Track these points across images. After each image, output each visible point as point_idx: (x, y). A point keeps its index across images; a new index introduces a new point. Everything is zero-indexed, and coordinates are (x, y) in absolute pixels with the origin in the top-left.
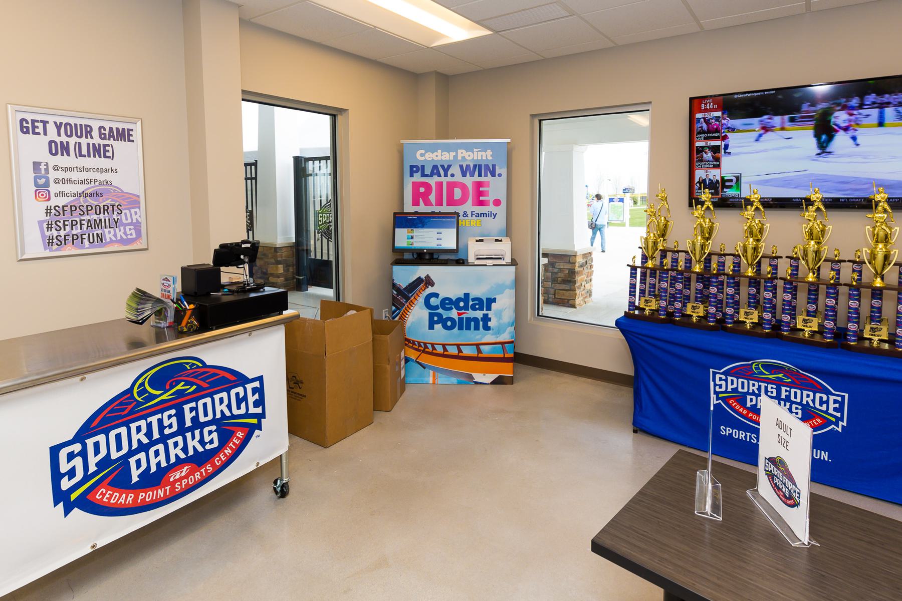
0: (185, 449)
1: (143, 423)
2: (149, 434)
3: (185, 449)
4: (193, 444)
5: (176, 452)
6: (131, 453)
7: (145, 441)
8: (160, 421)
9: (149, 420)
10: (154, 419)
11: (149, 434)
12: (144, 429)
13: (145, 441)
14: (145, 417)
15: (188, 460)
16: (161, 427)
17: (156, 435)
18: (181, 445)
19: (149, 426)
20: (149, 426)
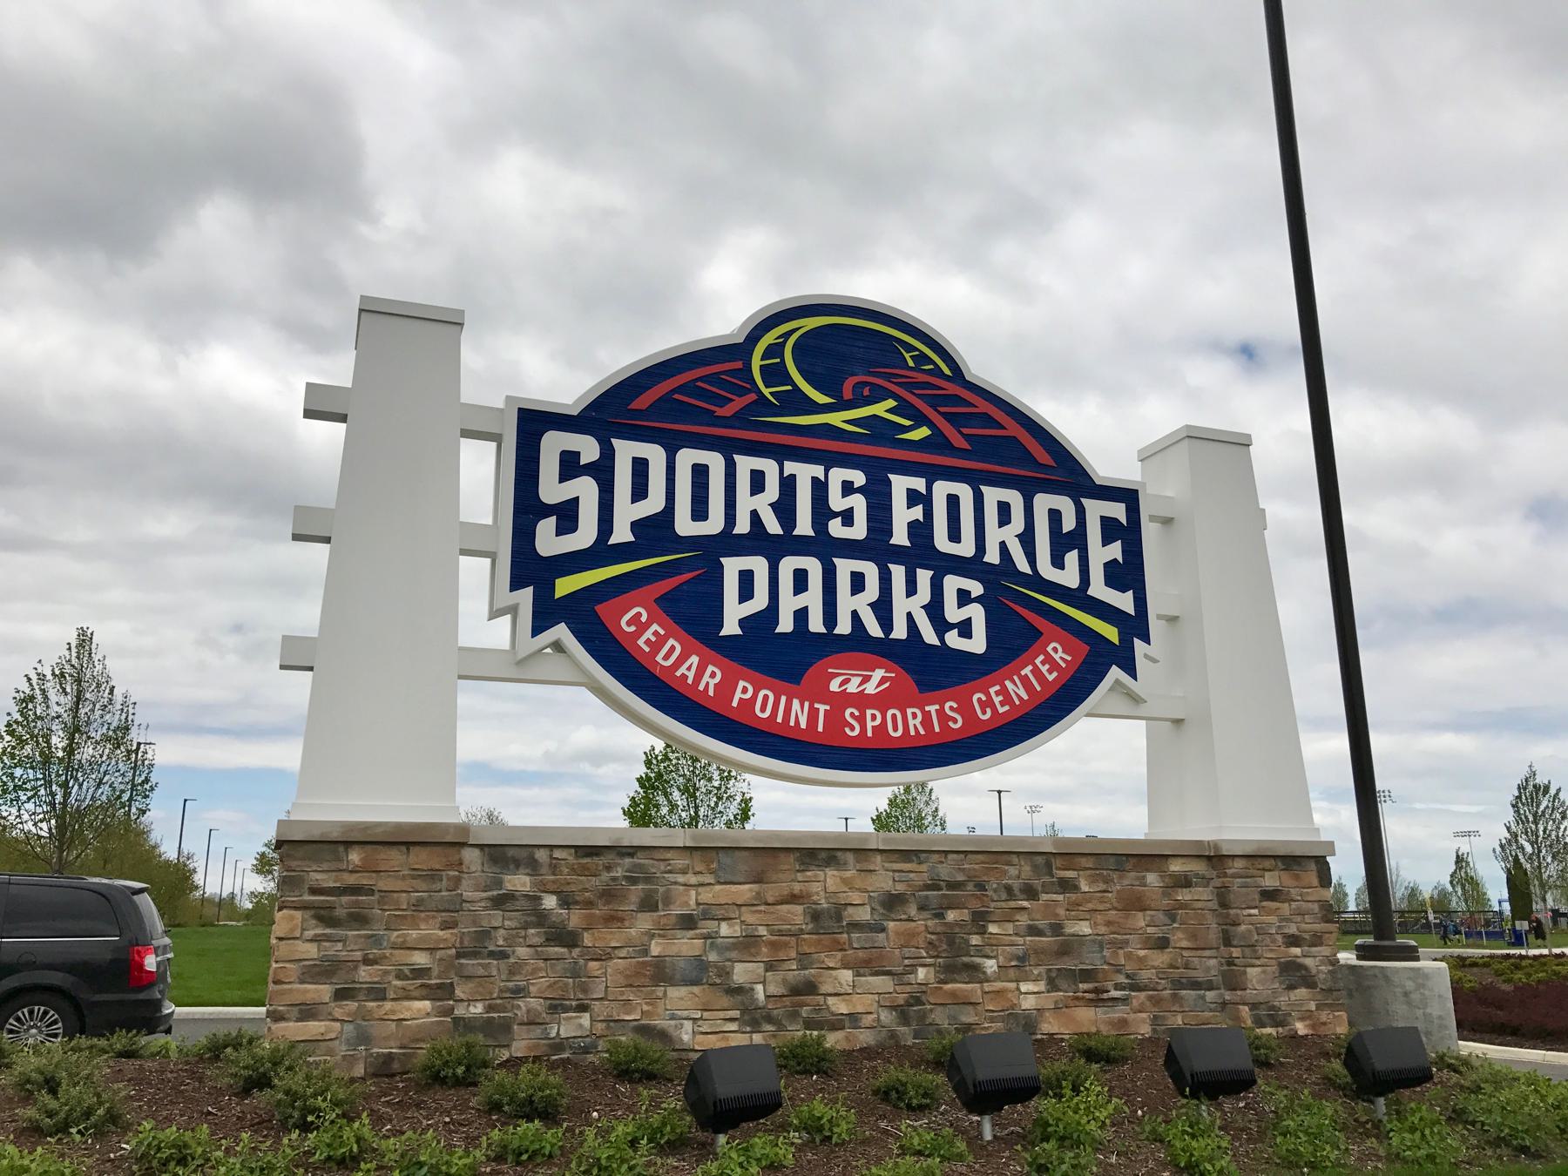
0: (883, 608)
1: (769, 466)
2: (785, 508)
4: (908, 607)
6: (728, 543)
7: (773, 526)
8: (820, 488)
9: (790, 467)
10: (805, 473)
11: (785, 508)
12: (772, 491)
13: (773, 526)
14: (781, 454)
15: (886, 650)
16: (822, 512)
17: (804, 527)
18: (872, 591)
19: (788, 484)
20: (788, 484)
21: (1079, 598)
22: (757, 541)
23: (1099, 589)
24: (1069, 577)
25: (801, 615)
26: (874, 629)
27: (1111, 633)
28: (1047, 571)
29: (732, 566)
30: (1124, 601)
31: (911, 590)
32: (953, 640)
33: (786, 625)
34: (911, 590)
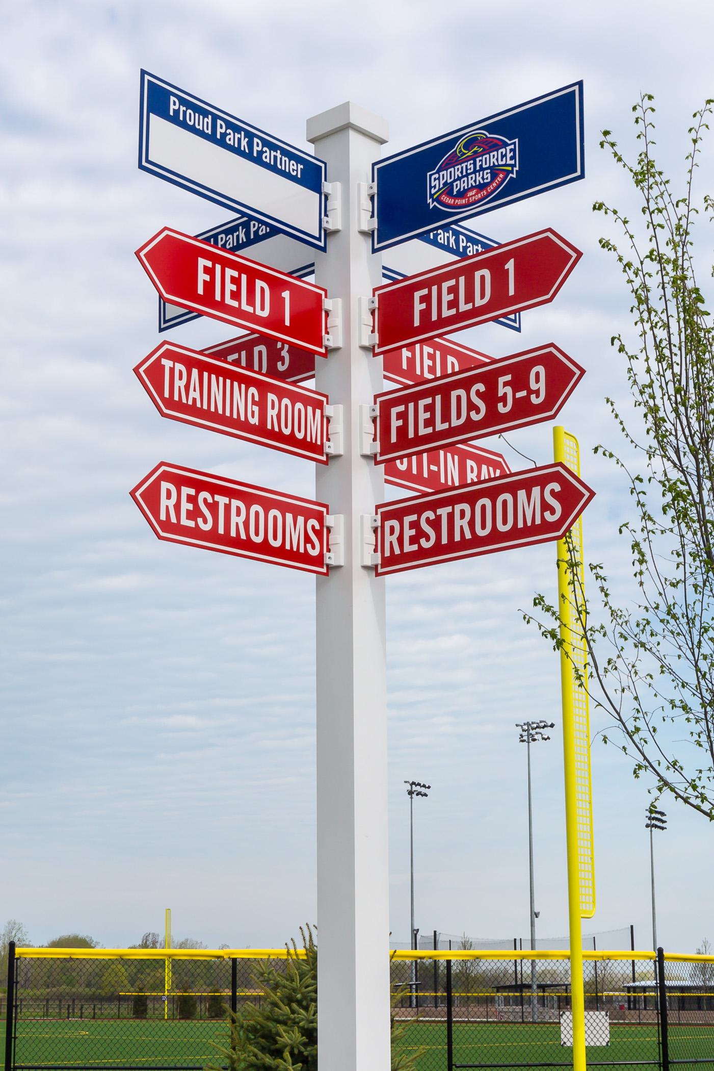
0: (475, 181)
3: (475, 181)
4: (479, 179)
5: (471, 182)
6: (455, 181)
7: (460, 175)
11: (462, 172)
13: (460, 175)
17: (464, 173)
21: (506, 165)
22: (459, 179)
23: (509, 162)
24: (504, 162)
25: (464, 187)
26: (474, 184)
27: (510, 168)
28: (500, 163)
29: (455, 184)
30: (513, 162)
31: (479, 176)
32: (485, 181)
33: (462, 189)
34: (479, 176)
